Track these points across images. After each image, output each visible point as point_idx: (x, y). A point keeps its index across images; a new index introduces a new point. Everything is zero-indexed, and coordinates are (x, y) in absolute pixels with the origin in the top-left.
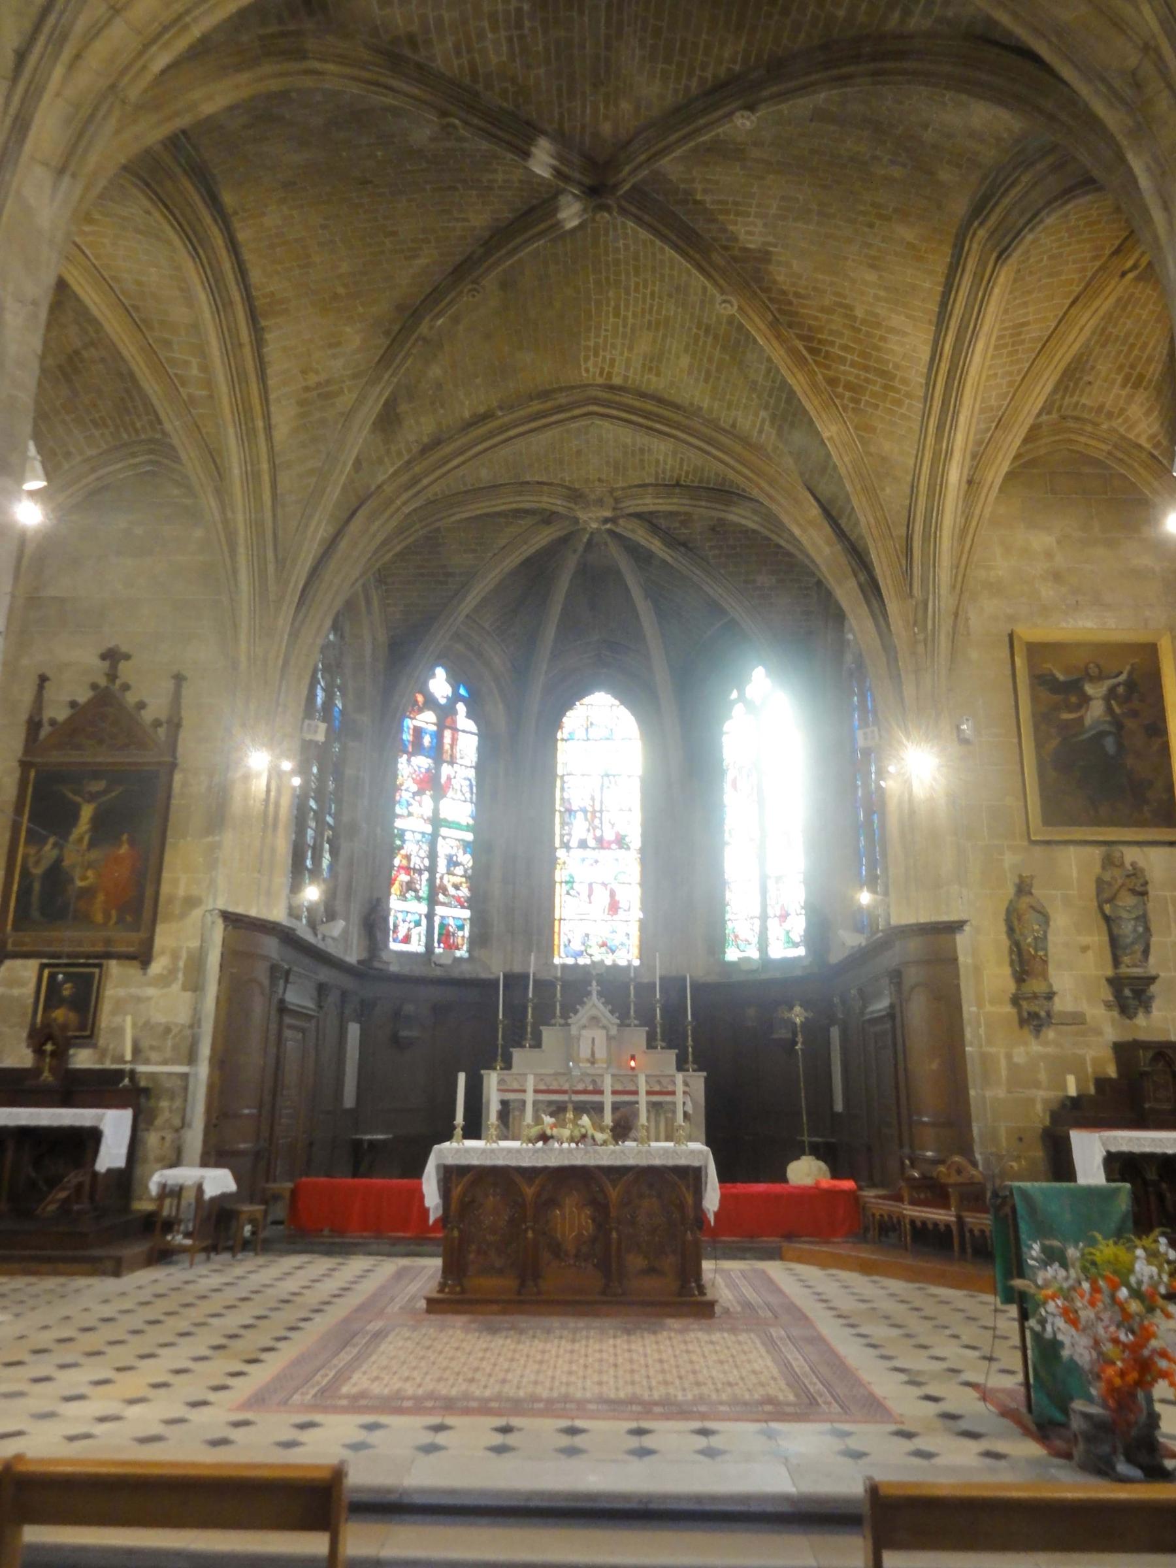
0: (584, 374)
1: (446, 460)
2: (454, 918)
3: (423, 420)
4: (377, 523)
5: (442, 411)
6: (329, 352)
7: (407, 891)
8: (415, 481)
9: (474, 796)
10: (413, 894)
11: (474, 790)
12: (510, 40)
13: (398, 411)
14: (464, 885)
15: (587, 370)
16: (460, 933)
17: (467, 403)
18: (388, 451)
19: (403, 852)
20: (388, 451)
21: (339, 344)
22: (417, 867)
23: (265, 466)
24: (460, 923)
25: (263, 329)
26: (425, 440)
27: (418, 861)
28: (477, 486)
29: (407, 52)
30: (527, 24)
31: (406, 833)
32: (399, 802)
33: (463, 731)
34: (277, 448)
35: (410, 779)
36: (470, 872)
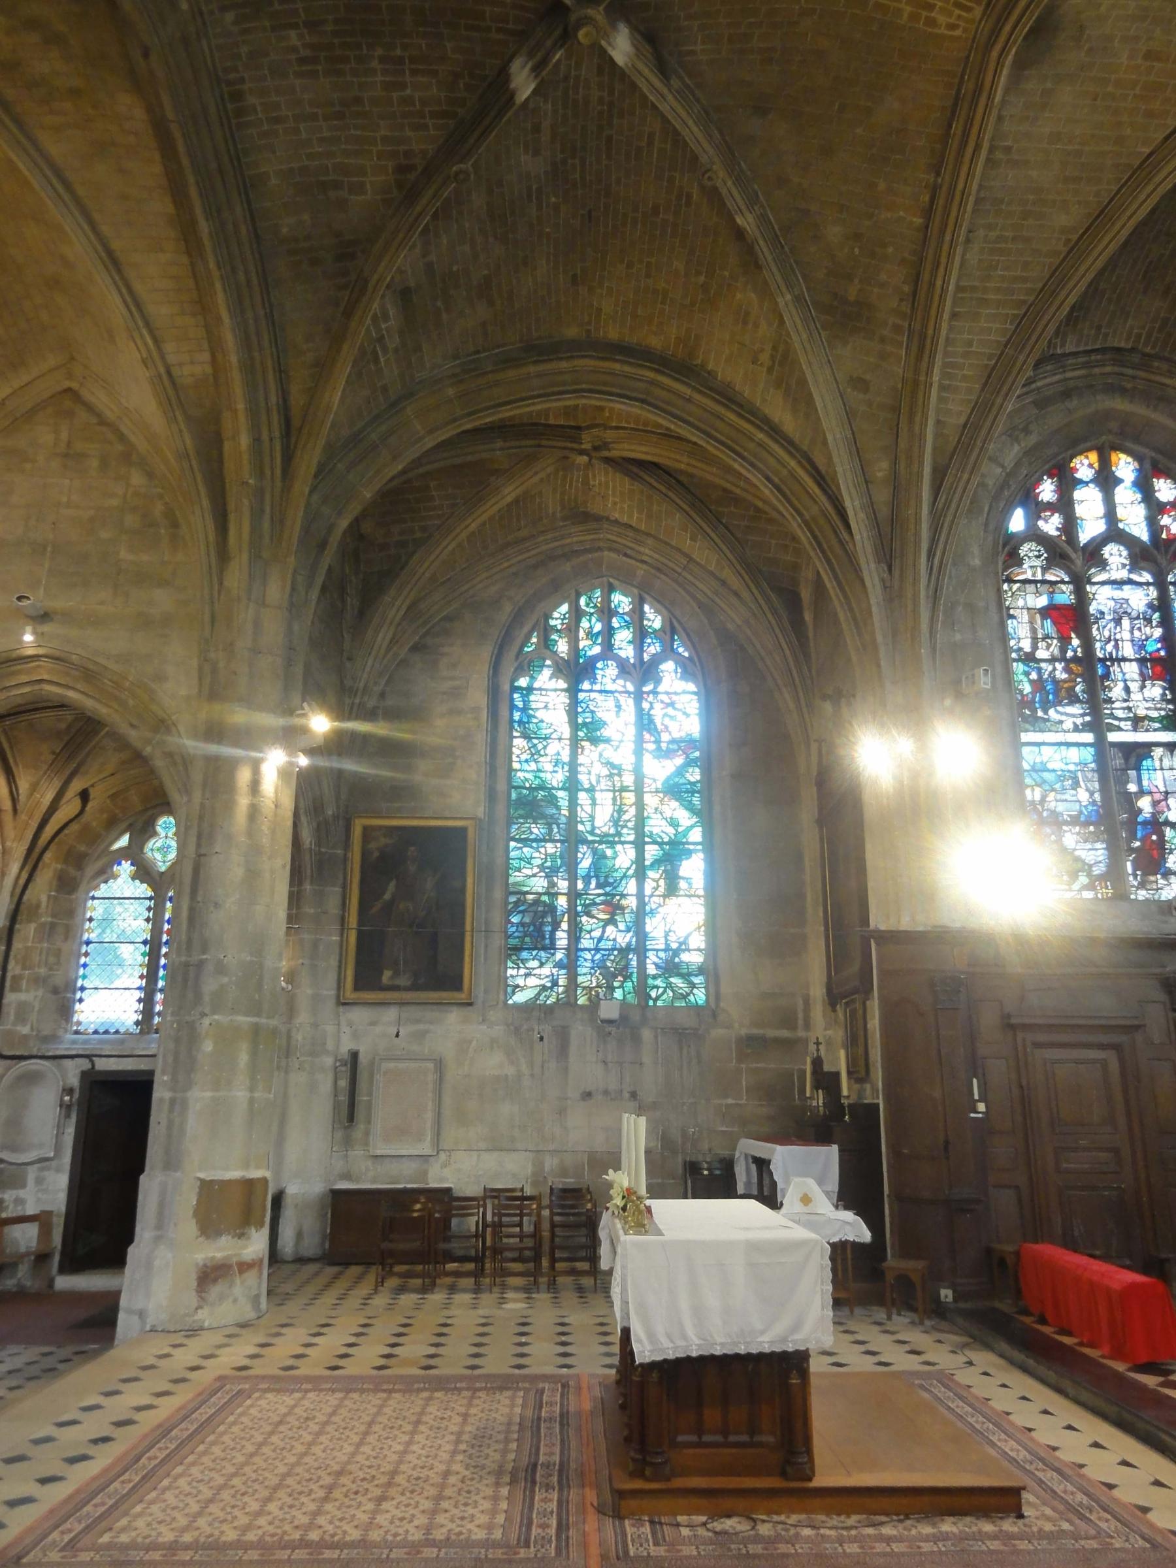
0: (958, 33)
1: (932, 285)
3: (883, 277)
4: (918, 419)
5: (890, 250)
6: (750, 326)
8: (923, 337)
12: (414, 72)
13: (852, 298)
15: (952, 27)
17: (901, 213)
18: (882, 340)
20: (882, 340)
21: (747, 314)
23: (793, 463)
25: (702, 366)
26: (906, 289)
28: (1075, 237)
29: (412, 176)
30: (398, 52)
34: (796, 438)
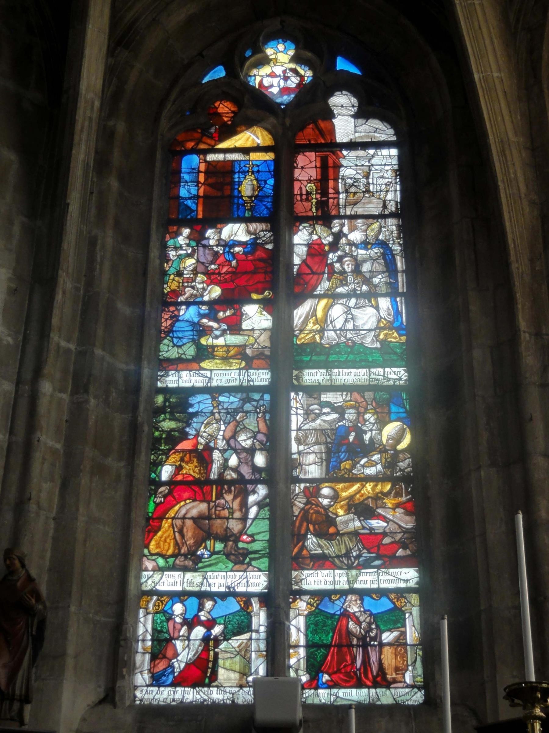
2: (362, 594)
7: (199, 543)
9: (401, 279)
10: (219, 546)
11: (400, 264)
14: (389, 502)
16: (387, 637)
19: (185, 445)
22: (231, 475)
24: (385, 604)
27: (233, 461)
31: (193, 400)
32: (170, 331)
33: (352, 145)
35: (200, 277)
36: (405, 464)
